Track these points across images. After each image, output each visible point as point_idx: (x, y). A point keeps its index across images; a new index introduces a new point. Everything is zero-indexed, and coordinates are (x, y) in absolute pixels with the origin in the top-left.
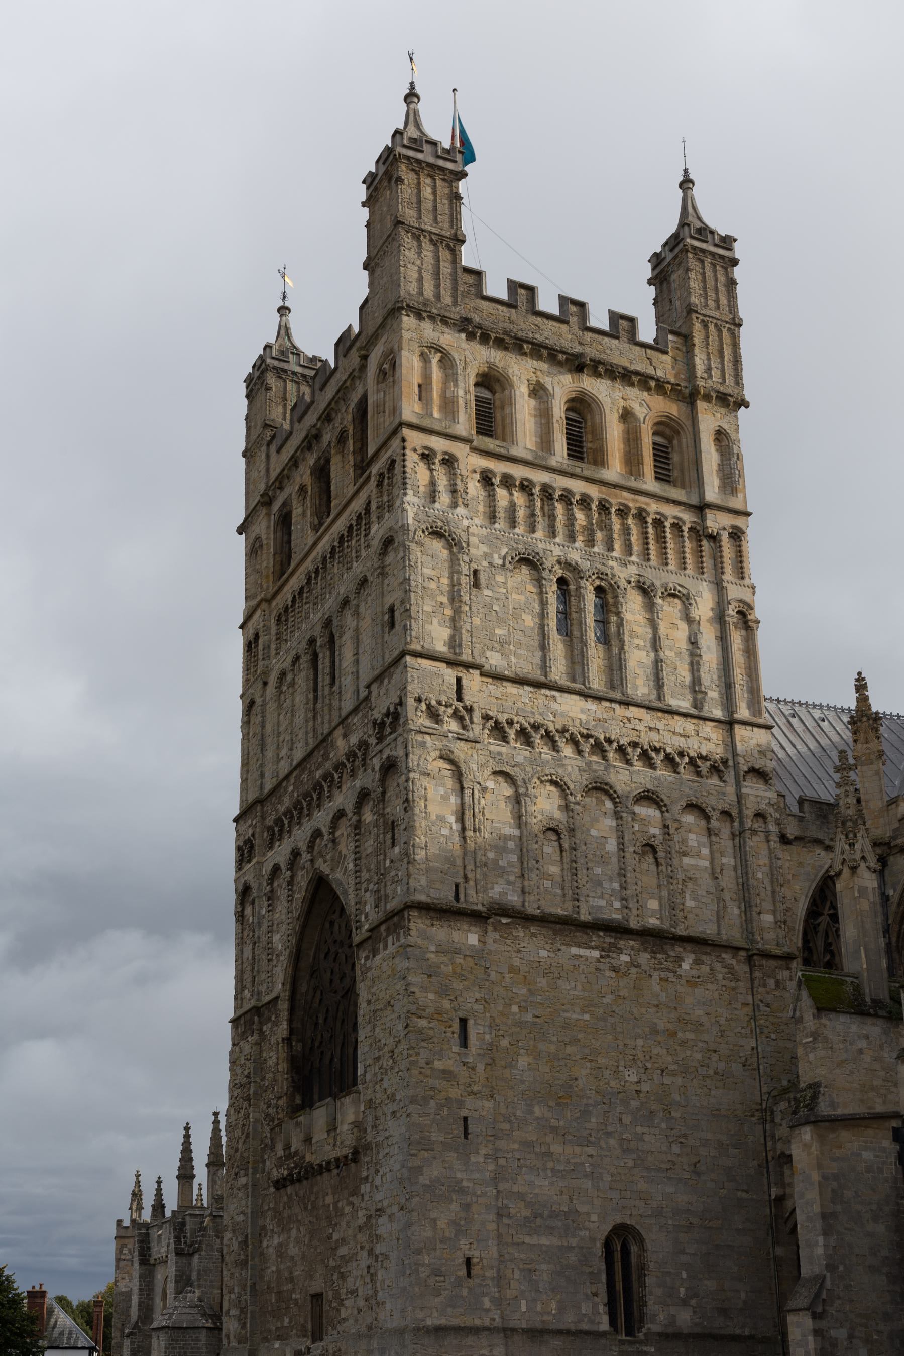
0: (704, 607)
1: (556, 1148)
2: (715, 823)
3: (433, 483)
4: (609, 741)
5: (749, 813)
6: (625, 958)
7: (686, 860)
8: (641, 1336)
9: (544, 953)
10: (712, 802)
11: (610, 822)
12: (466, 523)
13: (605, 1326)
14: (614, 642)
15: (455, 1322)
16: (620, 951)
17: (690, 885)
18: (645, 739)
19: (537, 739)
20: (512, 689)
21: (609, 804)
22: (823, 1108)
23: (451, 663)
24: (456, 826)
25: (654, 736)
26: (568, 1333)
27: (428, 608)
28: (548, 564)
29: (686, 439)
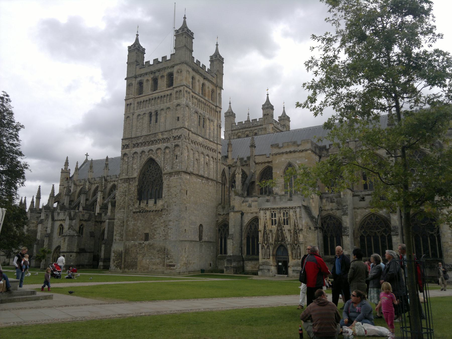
2: (214, 160)
3: (187, 97)
5: (218, 159)
6: (204, 181)
8: (201, 241)
10: (215, 157)
11: (203, 159)
13: (198, 240)
15: (184, 239)
18: (208, 145)
22: (235, 210)
23: (188, 130)
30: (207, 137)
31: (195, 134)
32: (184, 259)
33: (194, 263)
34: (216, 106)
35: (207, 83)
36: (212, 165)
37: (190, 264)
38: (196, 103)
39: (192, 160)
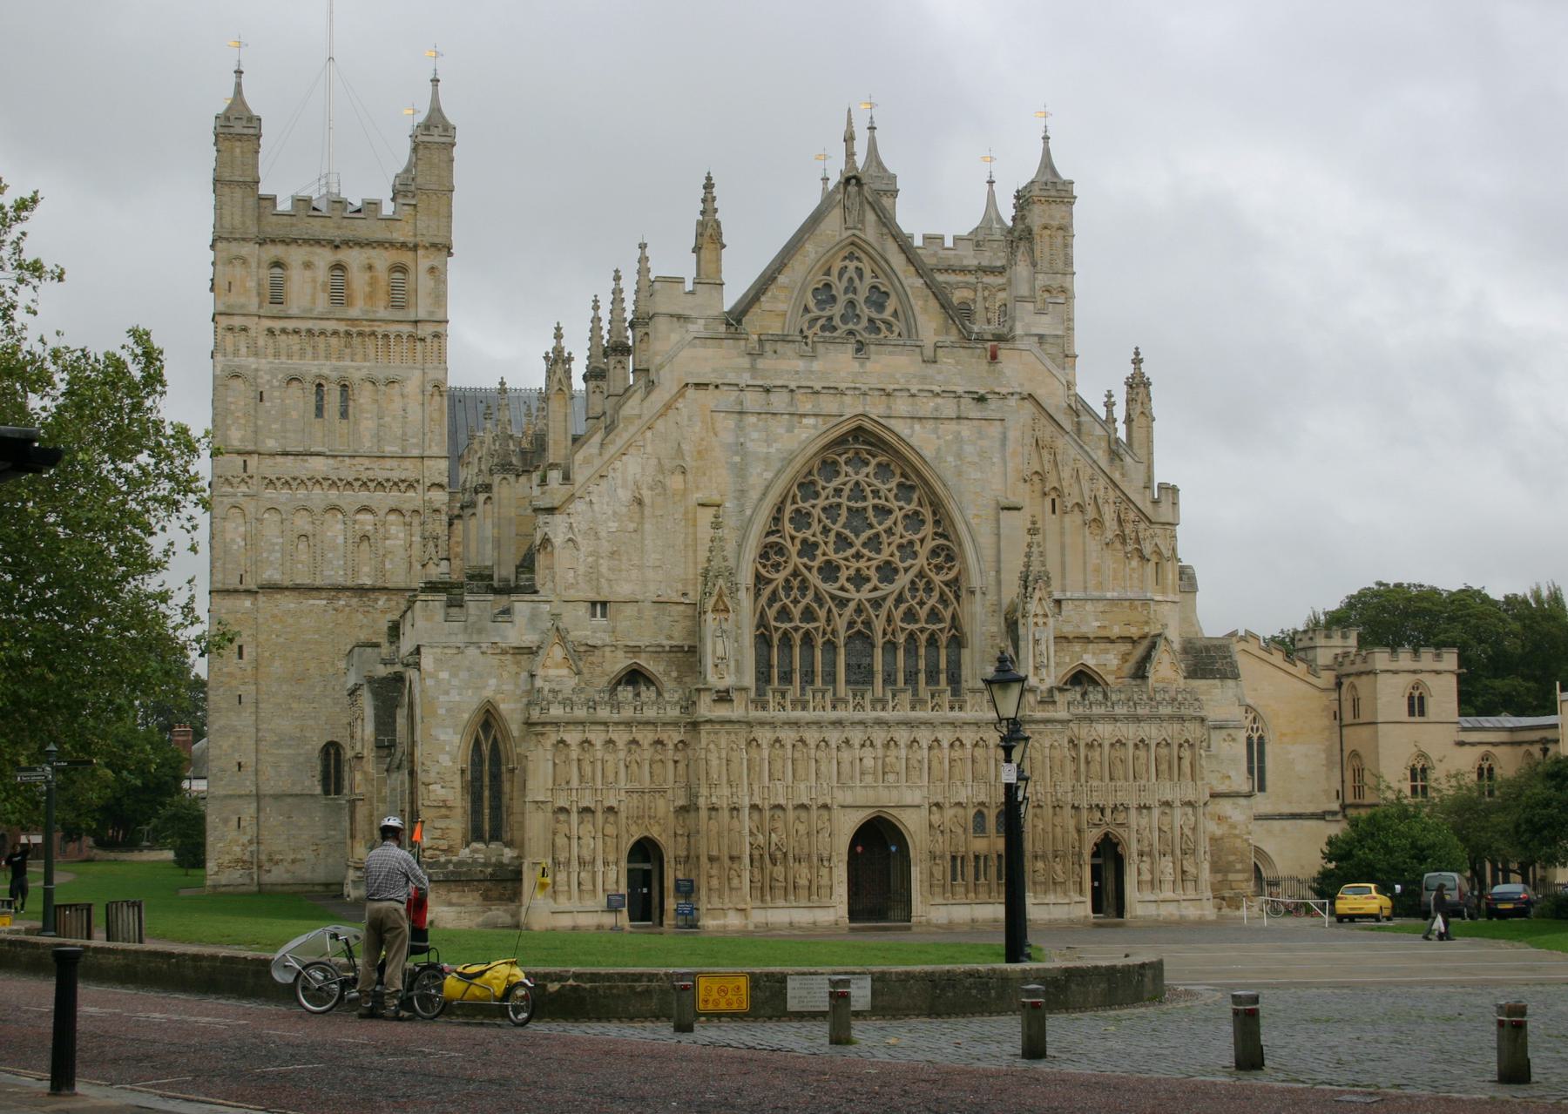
0: (413, 385)
1: (294, 705)
2: (408, 519)
4: (341, 480)
6: (342, 602)
7: (387, 542)
9: (292, 605)
10: (406, 507)
11: (340, 526)
12: (253, 366)
13: (318, 790)
14: (351, 417)
16: (339, 599)
17: (390, 556)
19: (294, 484)
20: (279, 459)
21: (340, 516)
23: (239, 453)
24: (243, 543)
25: (370, 474)
26: (297, 795)
27: (229, 422)
28: (308, 379)
29: (412, 277)
30: (367, 445)
31: (285, 454)
32: (237, 849)
33: (294, 861)
34: (416, 322)
35: (353, 257)
36: (397, 532)
37: (277, 863)
38: (296, 348)
39: (273, 544)
